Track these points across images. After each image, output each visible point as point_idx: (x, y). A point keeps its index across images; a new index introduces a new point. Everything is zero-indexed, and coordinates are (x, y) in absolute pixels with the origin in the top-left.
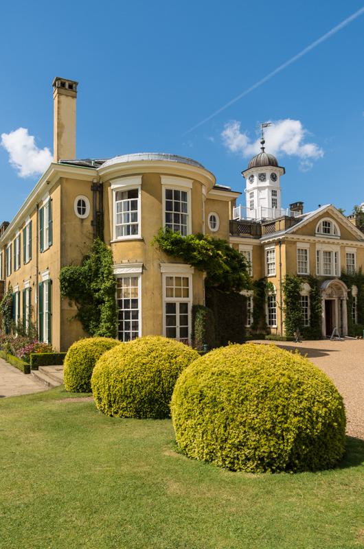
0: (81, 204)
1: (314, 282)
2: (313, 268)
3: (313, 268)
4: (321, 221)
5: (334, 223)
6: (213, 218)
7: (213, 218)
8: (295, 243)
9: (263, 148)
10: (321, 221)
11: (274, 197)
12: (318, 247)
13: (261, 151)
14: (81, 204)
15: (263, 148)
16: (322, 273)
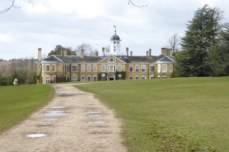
0: (39, 67)
1: (106, 74)
2: (106, 70)
3: (106, 70)
4: (110, 59)
5: (114, 59)
6: (60, 67)
7: (60, 67)
8: (101, 64)
9: (115, 33)
10: (110, 59)
11: (114, 48)
12: (108, 65)
13: (115, 34)
14: (39, 67)
15: (115, 33)
16: (109, 72)
